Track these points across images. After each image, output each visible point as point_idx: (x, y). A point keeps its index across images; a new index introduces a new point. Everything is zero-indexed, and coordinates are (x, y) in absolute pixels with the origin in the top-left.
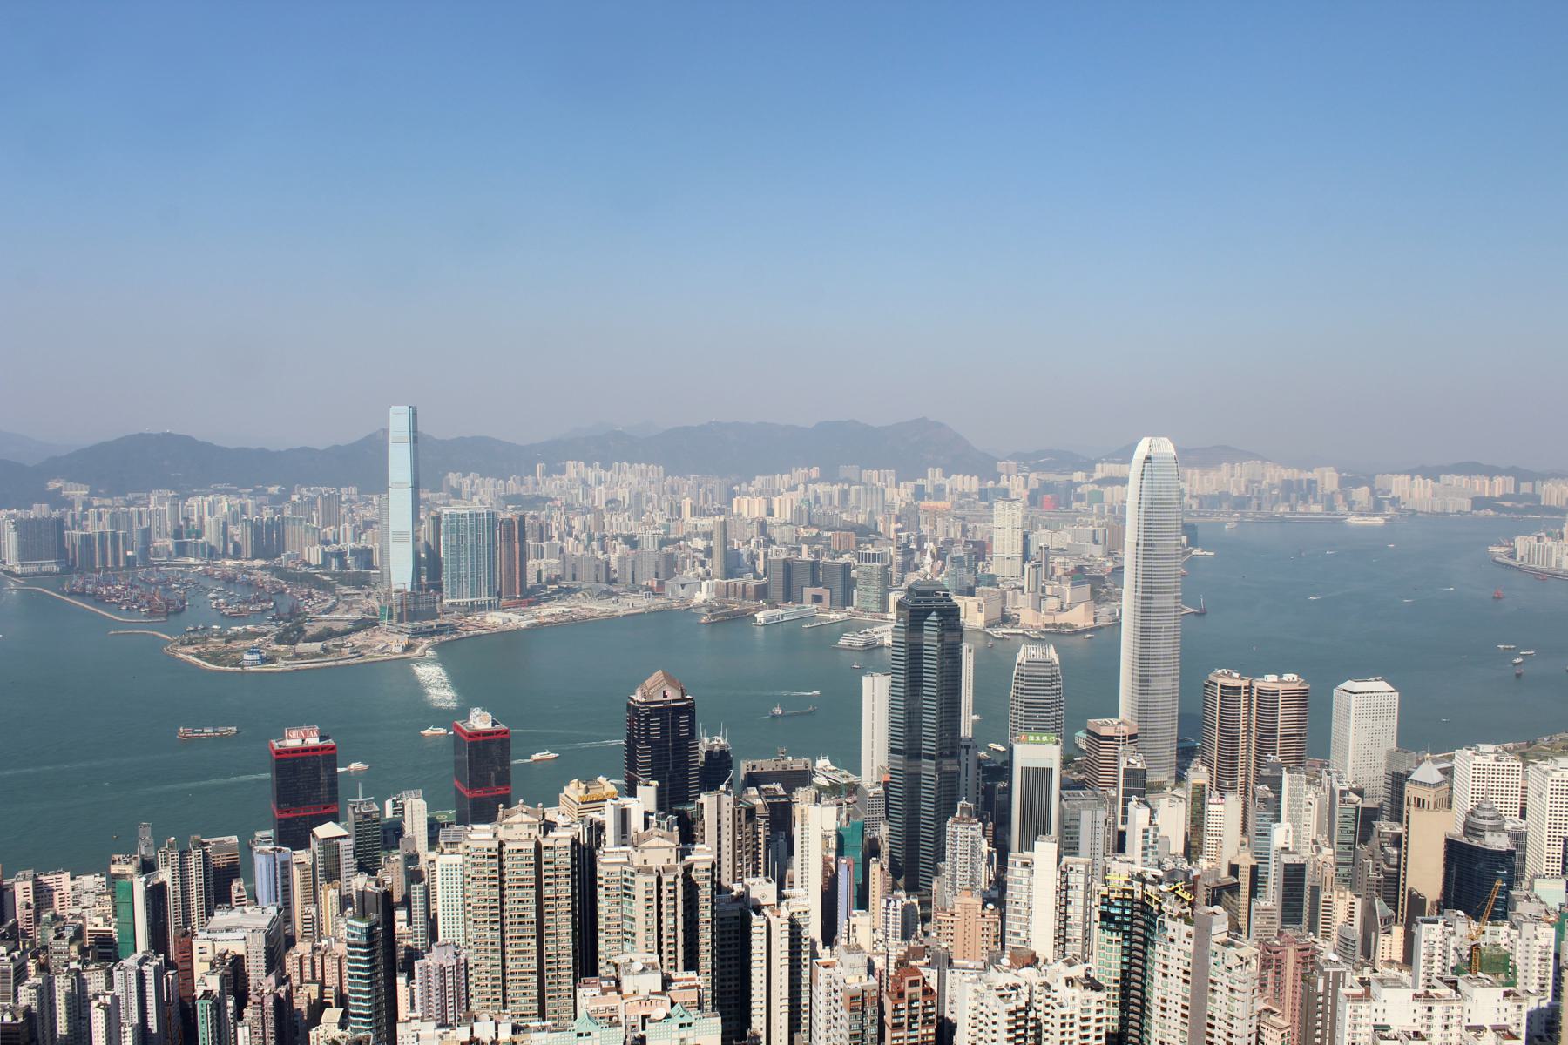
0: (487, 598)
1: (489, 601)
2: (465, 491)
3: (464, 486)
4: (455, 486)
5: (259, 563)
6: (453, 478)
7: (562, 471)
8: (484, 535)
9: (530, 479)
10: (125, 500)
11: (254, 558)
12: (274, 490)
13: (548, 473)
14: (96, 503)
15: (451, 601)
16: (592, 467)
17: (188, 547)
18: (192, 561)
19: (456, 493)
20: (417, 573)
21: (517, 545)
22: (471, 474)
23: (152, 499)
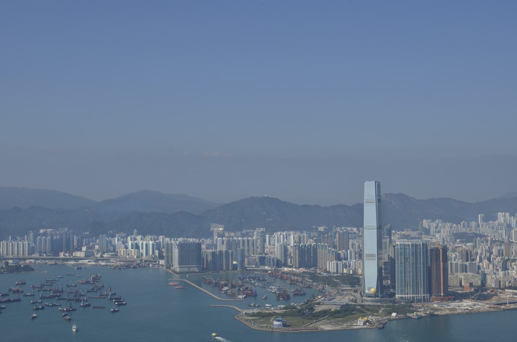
0: (422, 295)
1: (424, 297)
2: (432, 230)
3: (432, 227)
4: (427, 227)
5: (302, 270)
6: (425, 223)
7: (495, 218)
8: (420, 257)
9: (473, 224)
10: (241, 234)
11: (299, 267)
12: (321, 229)
13: (486, 220)
14: (227, 235)
15: (400, 296)
16: (514, 216)
17: (266, 260)
18: (266, 267)
19: (427, 232)
20: (380, 278)
21: (441, 263)
22: (437, 221)
23: (255, 233)
